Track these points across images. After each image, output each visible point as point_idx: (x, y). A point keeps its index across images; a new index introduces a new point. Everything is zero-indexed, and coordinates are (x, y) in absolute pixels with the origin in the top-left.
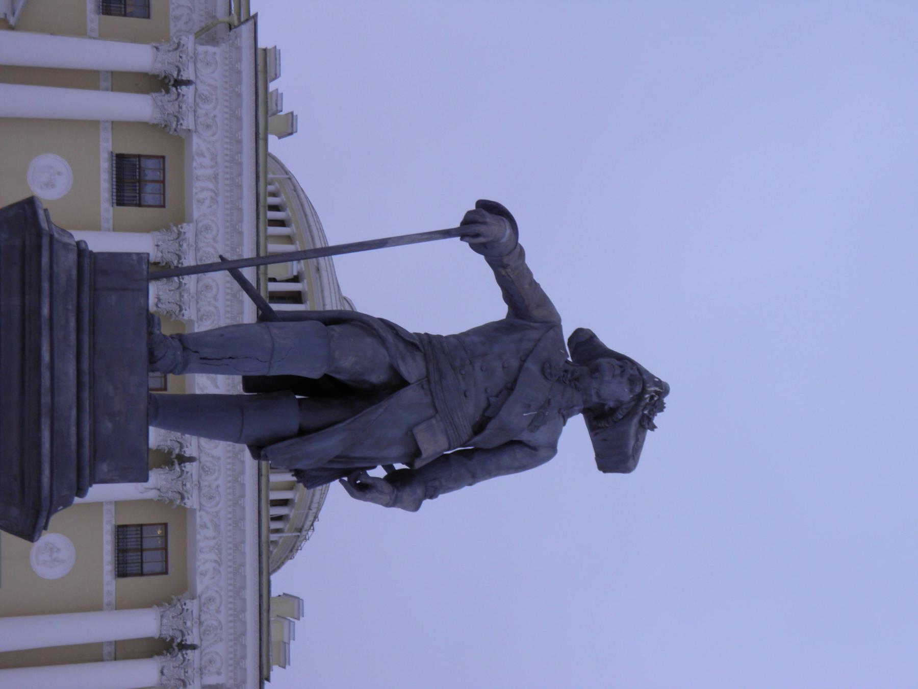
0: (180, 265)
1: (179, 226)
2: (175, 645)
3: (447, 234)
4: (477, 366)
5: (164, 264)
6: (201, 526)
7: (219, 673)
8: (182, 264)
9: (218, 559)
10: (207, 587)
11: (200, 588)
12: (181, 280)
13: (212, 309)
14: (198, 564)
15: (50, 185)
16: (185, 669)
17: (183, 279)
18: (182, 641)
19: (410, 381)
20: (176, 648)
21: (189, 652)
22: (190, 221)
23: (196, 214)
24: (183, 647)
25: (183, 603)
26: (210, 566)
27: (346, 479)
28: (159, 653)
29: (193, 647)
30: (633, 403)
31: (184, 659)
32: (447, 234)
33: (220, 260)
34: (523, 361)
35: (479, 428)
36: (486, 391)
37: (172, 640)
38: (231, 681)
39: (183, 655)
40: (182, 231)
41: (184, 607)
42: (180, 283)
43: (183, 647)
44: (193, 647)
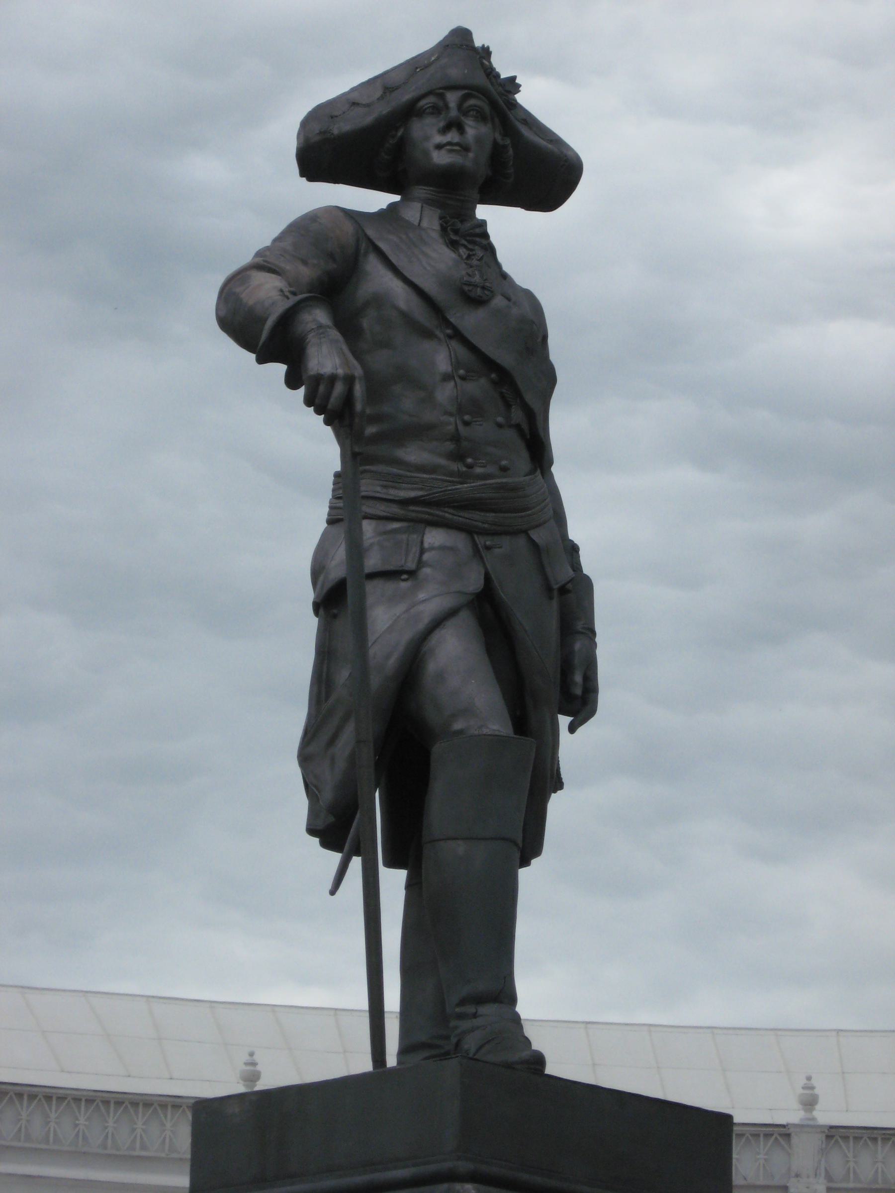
34: (458, 335)
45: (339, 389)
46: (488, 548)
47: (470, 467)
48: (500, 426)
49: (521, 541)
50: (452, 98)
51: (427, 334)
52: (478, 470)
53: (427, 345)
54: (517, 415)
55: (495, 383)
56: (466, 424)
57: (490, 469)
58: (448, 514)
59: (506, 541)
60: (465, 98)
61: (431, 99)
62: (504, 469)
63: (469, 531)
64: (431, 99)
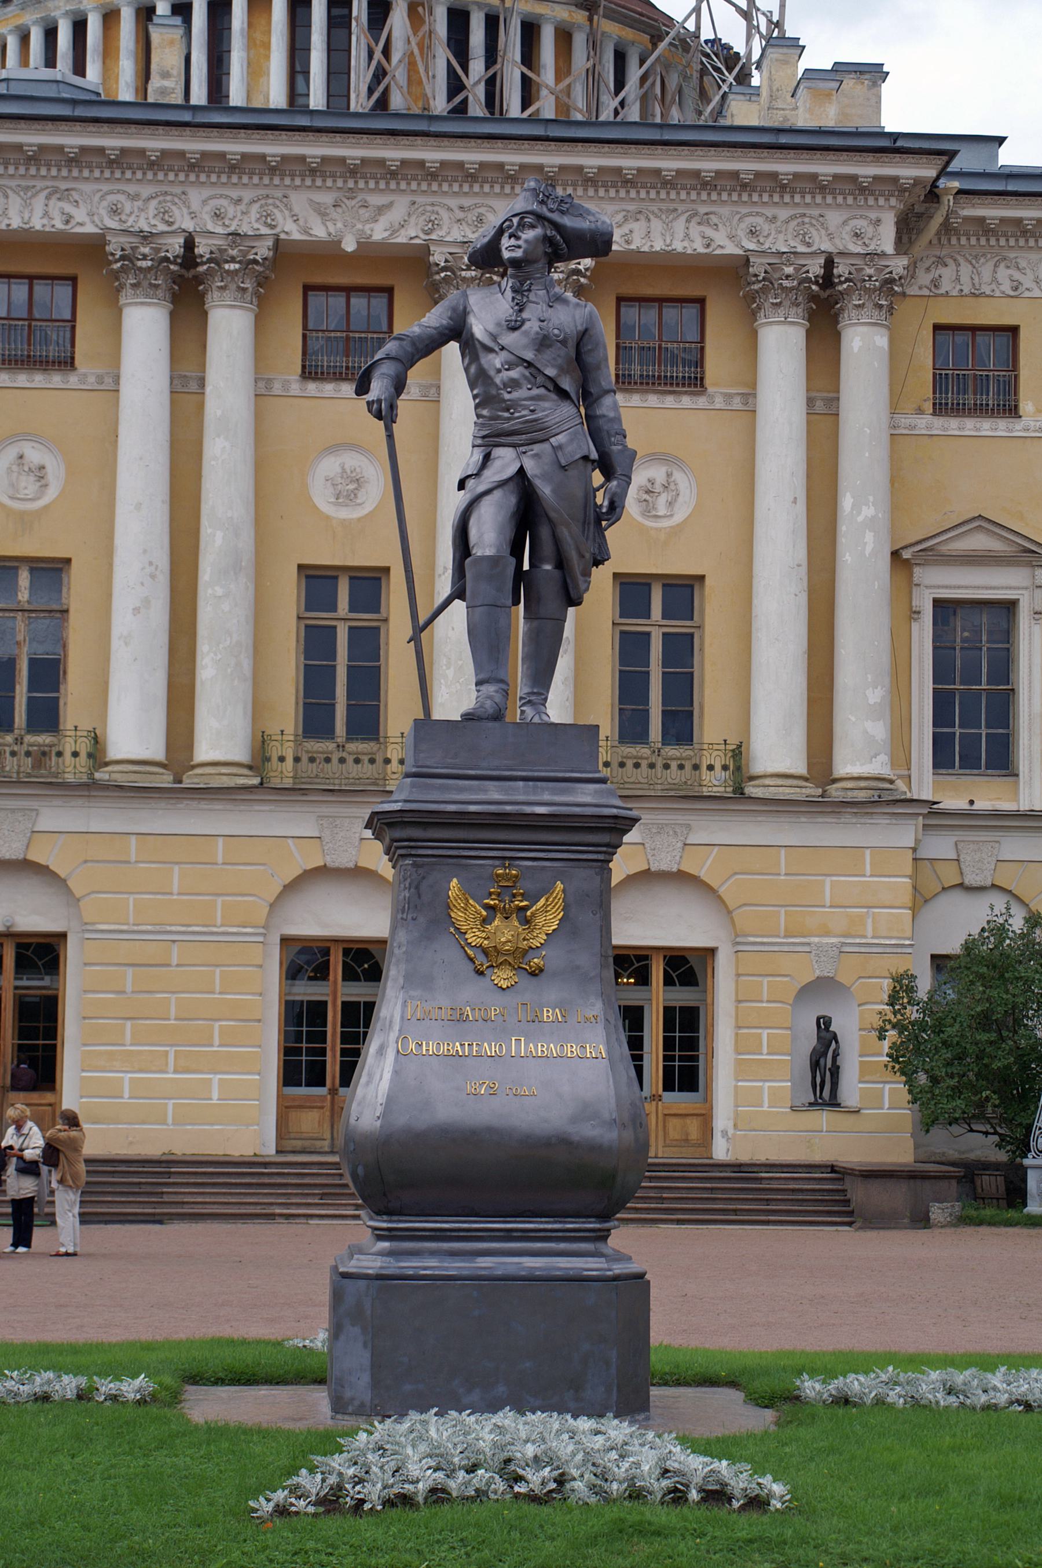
0: (179, 261)
1: (110, 258)
2: (824, 295)
3: (390, 437)
4: (507, 396)
5: (176, 288)
6: (628, 242)
7: (878, 222)
8: (177, 256)
9: (683, 218)
10: (731, 237)
11: (731, 249)
12: (204, 259)
13: (255, 207)
14: (689, 251)
15: (40, 473)
16: (865, 280)
17: (202, 256)
18: (817, 283)
19: (519, 465)
20: (828, 292)
21: (835, 271)
22: (103, 236)
23: (90, 229)
24: (827, 280)
25: (754, 279)
26: (695, 230)
27: (604, 523)
28: (835, 320)
29: (829, 263)
30: (546, 223)
31: (847, 280)
32: (390, 437)
33: (412, 643)
34: (503, 348)
35: (563, 394)
36: (530, 389)
37: (813, 298)
38: (893, 201)
39: (841, 283)
40: (119, 253)
41: (760, 278)
42: (210, 261)
43: (827, 280)
44: (829, 263)
45: (375, 406)
46: (524, 453)
47: (512, 414)
48: (530, 389)
49: (545, 446)
50: (515, 220)
51: (490, 350)
52: (517, 415)
53: (491, 356)
54: (540, 379)
55: (526, 368)
56: (509, 392)
57: (524, 413)
58: (502, 440)
59: (537, 448)
60: (522, 218)
61: (507, 223)
62: (532, 411)
63: (514, 446)
64: (507, 223)
